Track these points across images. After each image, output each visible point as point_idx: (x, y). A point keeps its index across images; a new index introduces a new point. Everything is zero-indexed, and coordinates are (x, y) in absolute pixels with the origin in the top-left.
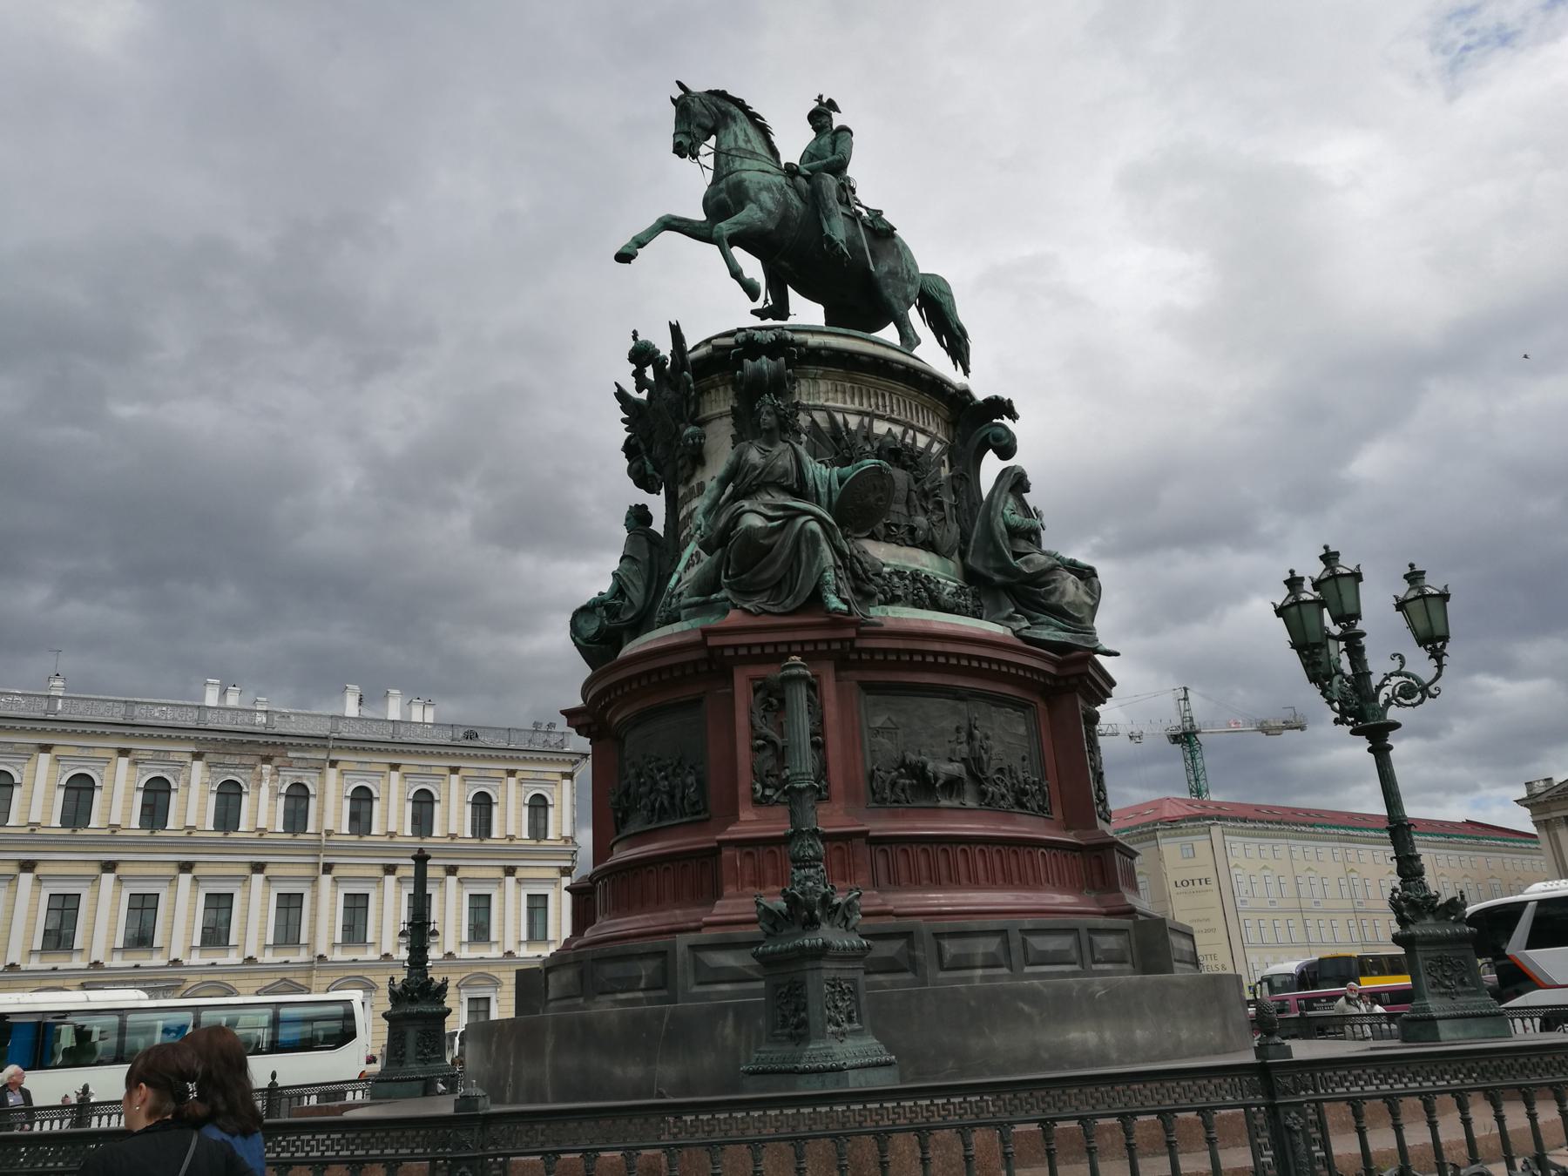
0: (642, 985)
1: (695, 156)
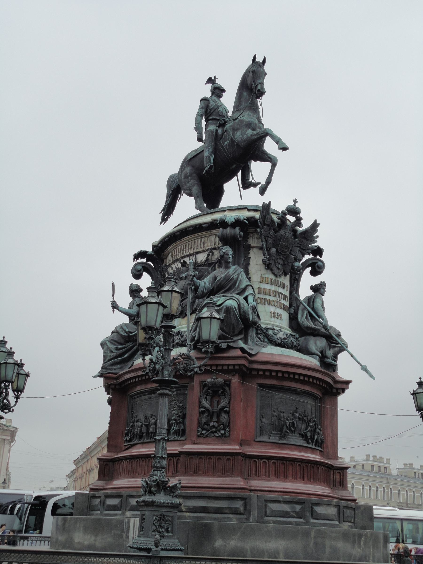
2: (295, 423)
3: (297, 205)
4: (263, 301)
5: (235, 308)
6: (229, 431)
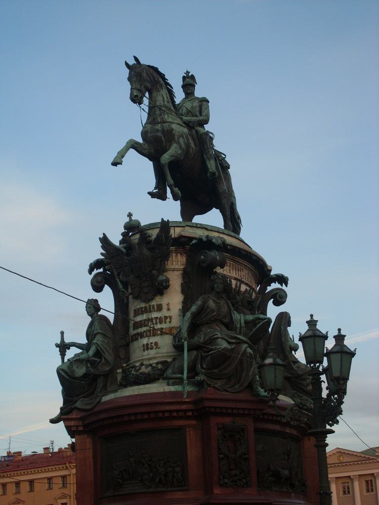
1: (140, 103)
3: (133, 218)
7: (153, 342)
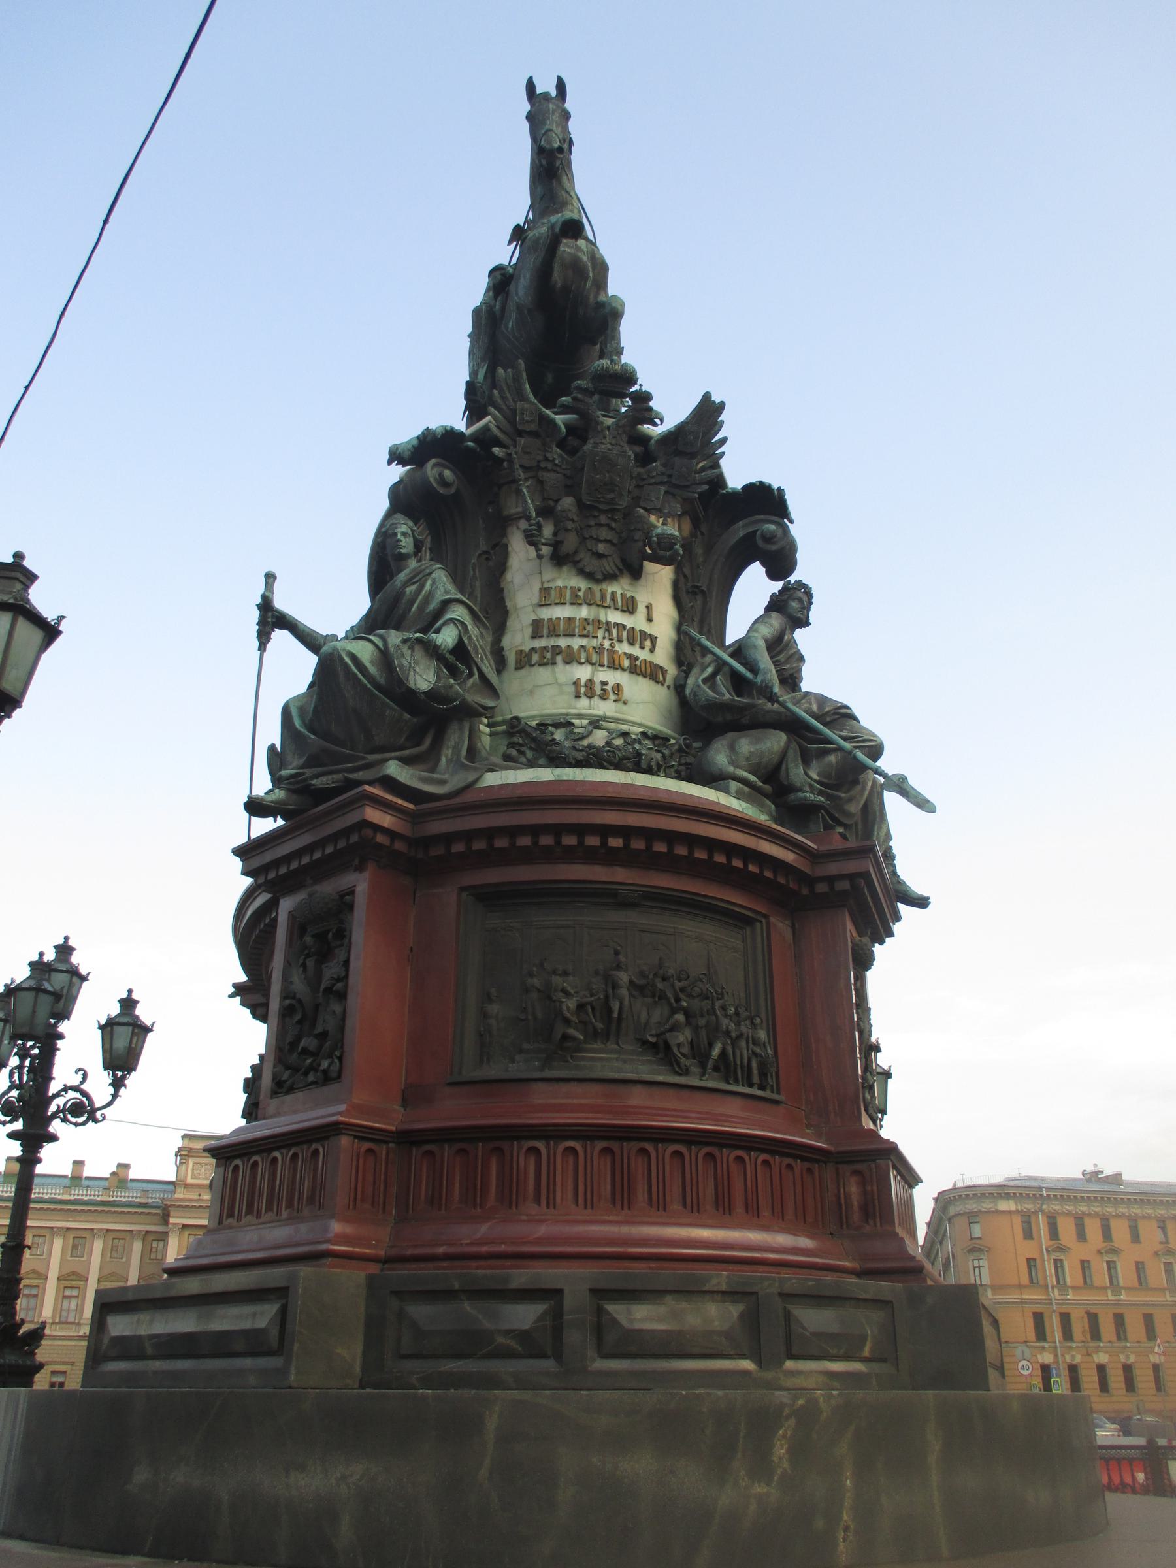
0: (866, 1352)
2: (615, 1006)
4: (549, 655)
5: (353, 657)
6: (340, 1058)
7: (611, 684)
